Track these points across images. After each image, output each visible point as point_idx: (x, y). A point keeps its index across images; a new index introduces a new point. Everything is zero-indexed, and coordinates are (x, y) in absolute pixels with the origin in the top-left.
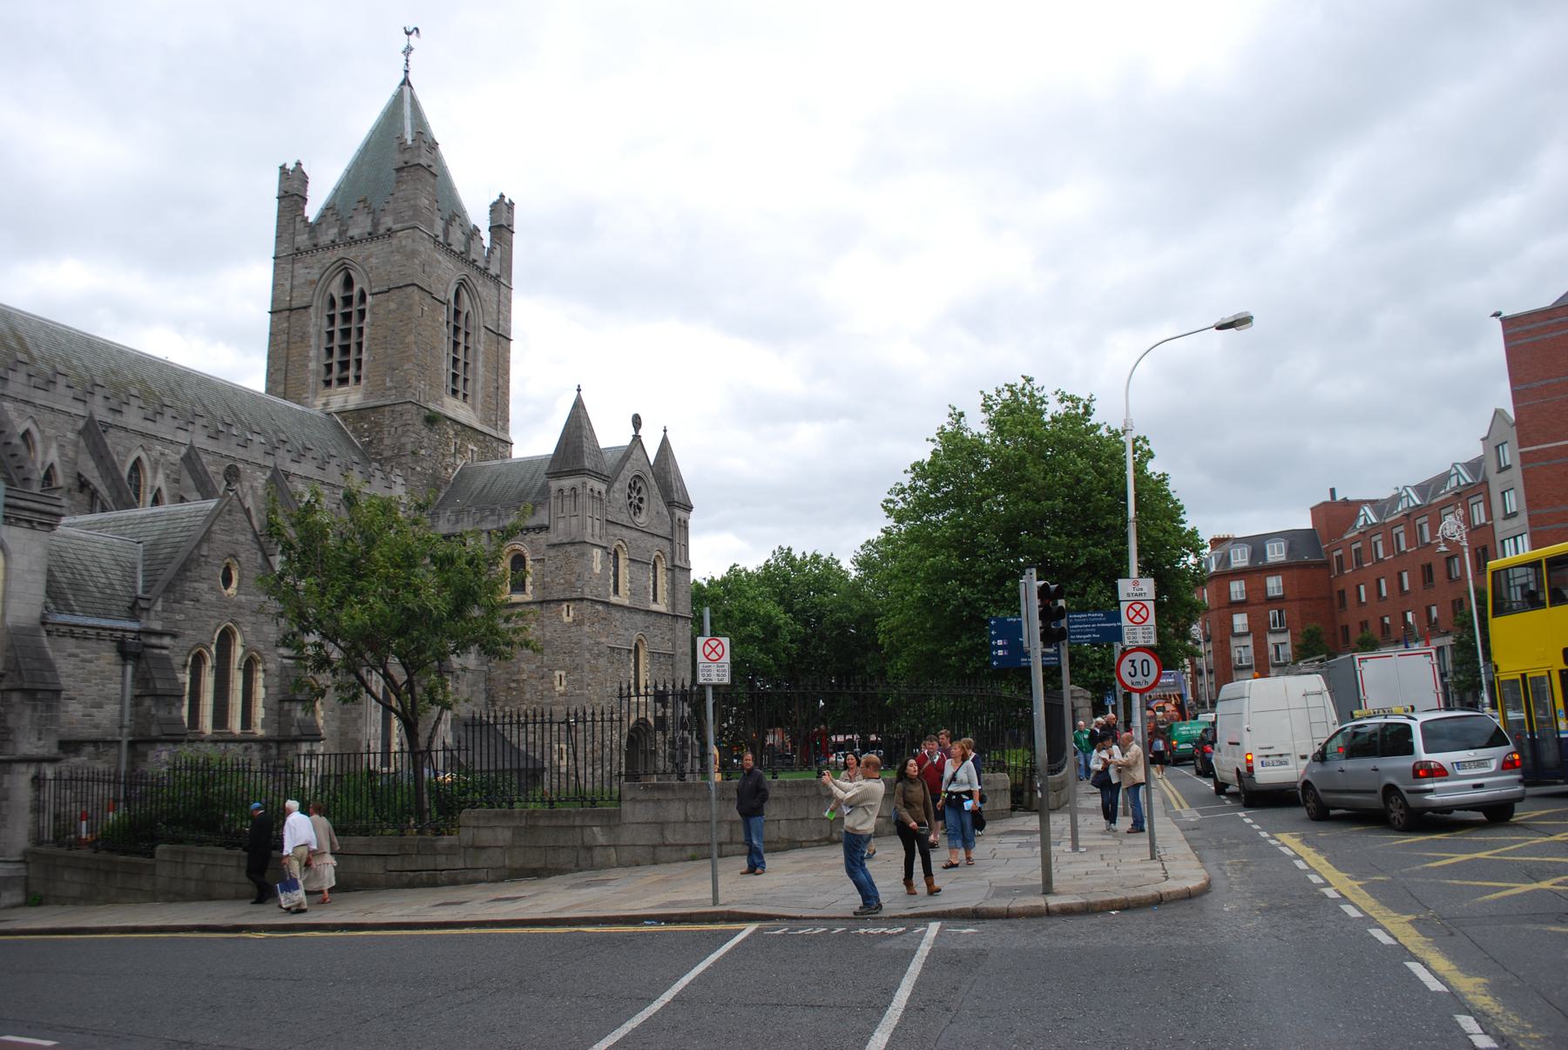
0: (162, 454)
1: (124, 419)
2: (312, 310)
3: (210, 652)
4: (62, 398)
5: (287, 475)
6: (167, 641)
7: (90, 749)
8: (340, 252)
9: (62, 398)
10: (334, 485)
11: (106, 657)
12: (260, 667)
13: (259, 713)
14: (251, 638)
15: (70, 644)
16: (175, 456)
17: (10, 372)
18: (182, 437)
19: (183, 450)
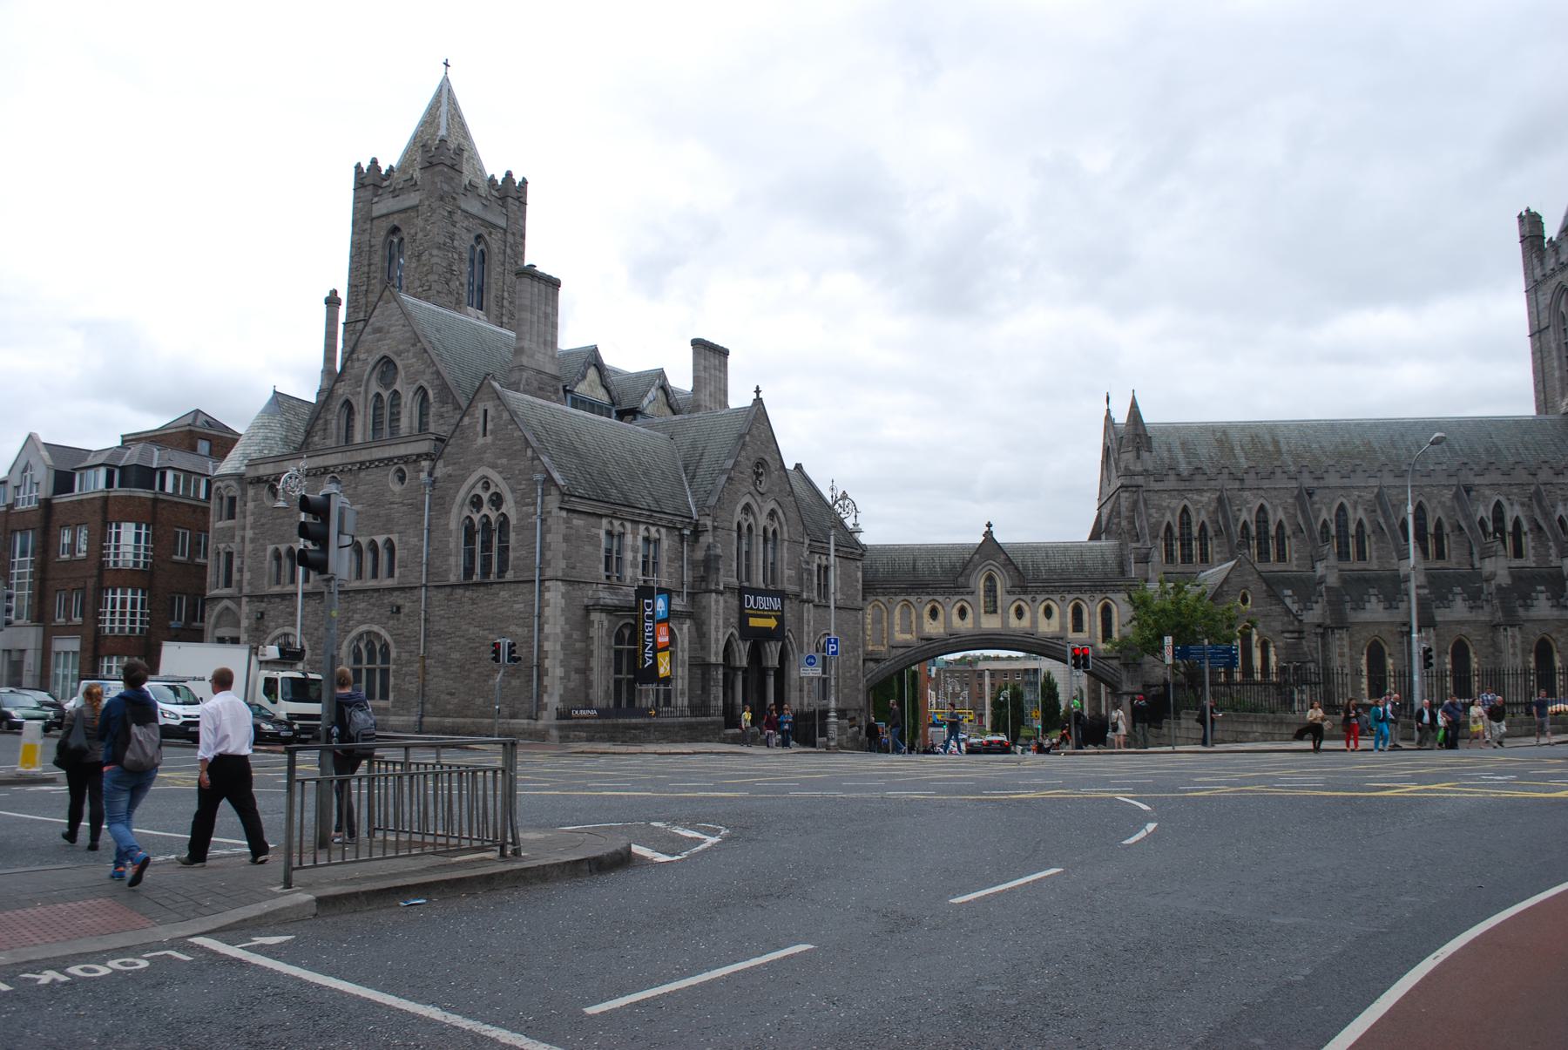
0: (1359, 497)
2: (1551, 329)
4: (1281, 482)
5: (1468, 489)
8: (1559, 278)
9: (1281, 482)
10: (1522, 484)
12: (1271, 645)
16: (1369, 496)
18: (1372, 482)
19: (1376, 490)
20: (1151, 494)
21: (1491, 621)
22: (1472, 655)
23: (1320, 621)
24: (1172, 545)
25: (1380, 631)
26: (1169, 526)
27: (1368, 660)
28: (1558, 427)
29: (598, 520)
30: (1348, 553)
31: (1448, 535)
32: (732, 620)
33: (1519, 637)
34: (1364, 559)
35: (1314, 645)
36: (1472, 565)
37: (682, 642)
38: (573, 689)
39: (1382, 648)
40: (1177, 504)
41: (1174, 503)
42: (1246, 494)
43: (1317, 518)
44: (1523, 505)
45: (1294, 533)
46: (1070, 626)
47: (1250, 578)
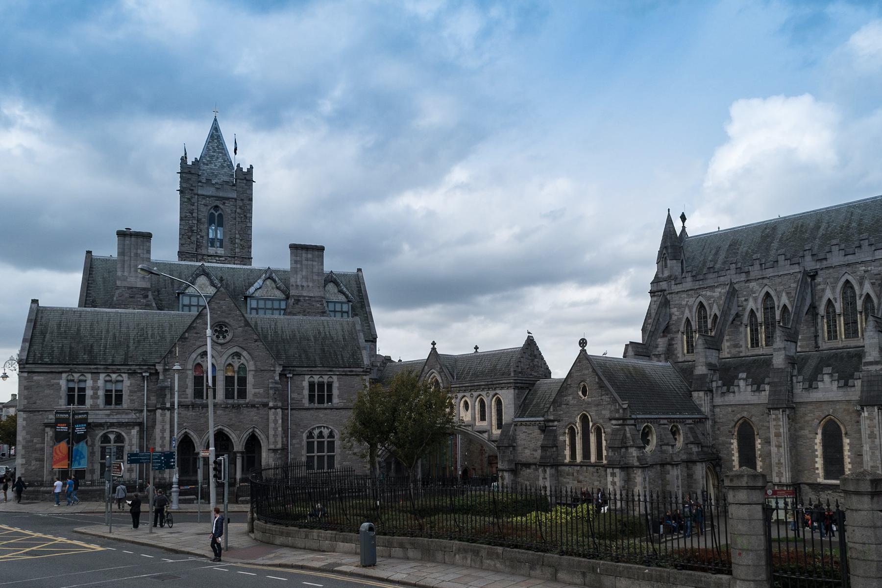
1: (828, 262)
3: (577, 427)
6: (556, 423)
7: (534, 467)
9: (784, 268)
11: (536, 432)
13: (604, 453)
14: (596, 418)
15: (524, 428)
17: (750, 267)
20: (673, 295)
24: (692, 337)
25: (834, 411)
26: (688, 321)
29: (60, 375)
32: (184, 425)
37: (130, 440)
38: (33, 470)
39: (839, 427)
40: (693, 302)
41: (691, 301)
42: (753, 285)
43: (821, 298)
46: (478, 416)
47: (586, 372)
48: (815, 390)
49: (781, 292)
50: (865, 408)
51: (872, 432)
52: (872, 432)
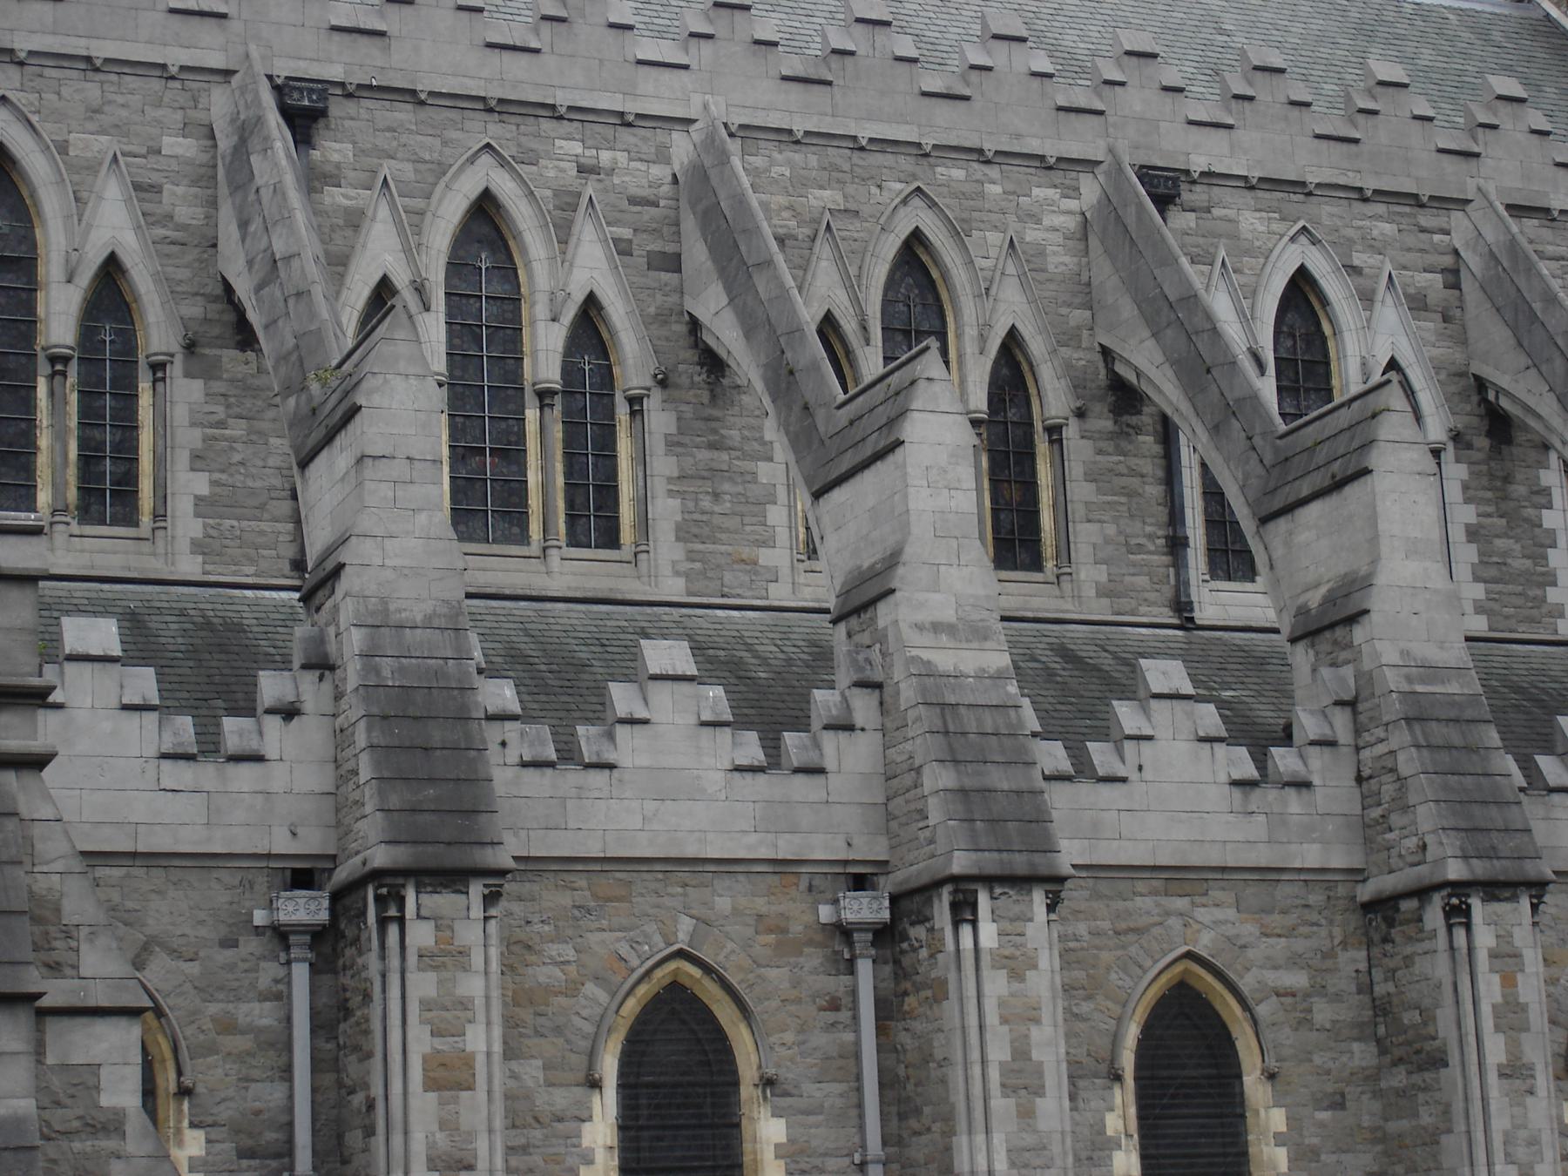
10: (1415, 200)
21: (1357, 875)
22: (1254, 1086)
23: (312, 842)
27: (628, 1125)
28: (1497, 36)
30: (519, 489)
31: (1054, 432)
33: (1532, 959)
34: (610, 539)
35: (262, 1015)
36: (1182, 607)
43: (338, 264)
44: (1417, 304)
45: (190, 347)
48: (598, 778)
49: (92, 168)
50: (983, 900)
51: (1021, 1052)
52: (1021, 1052)
